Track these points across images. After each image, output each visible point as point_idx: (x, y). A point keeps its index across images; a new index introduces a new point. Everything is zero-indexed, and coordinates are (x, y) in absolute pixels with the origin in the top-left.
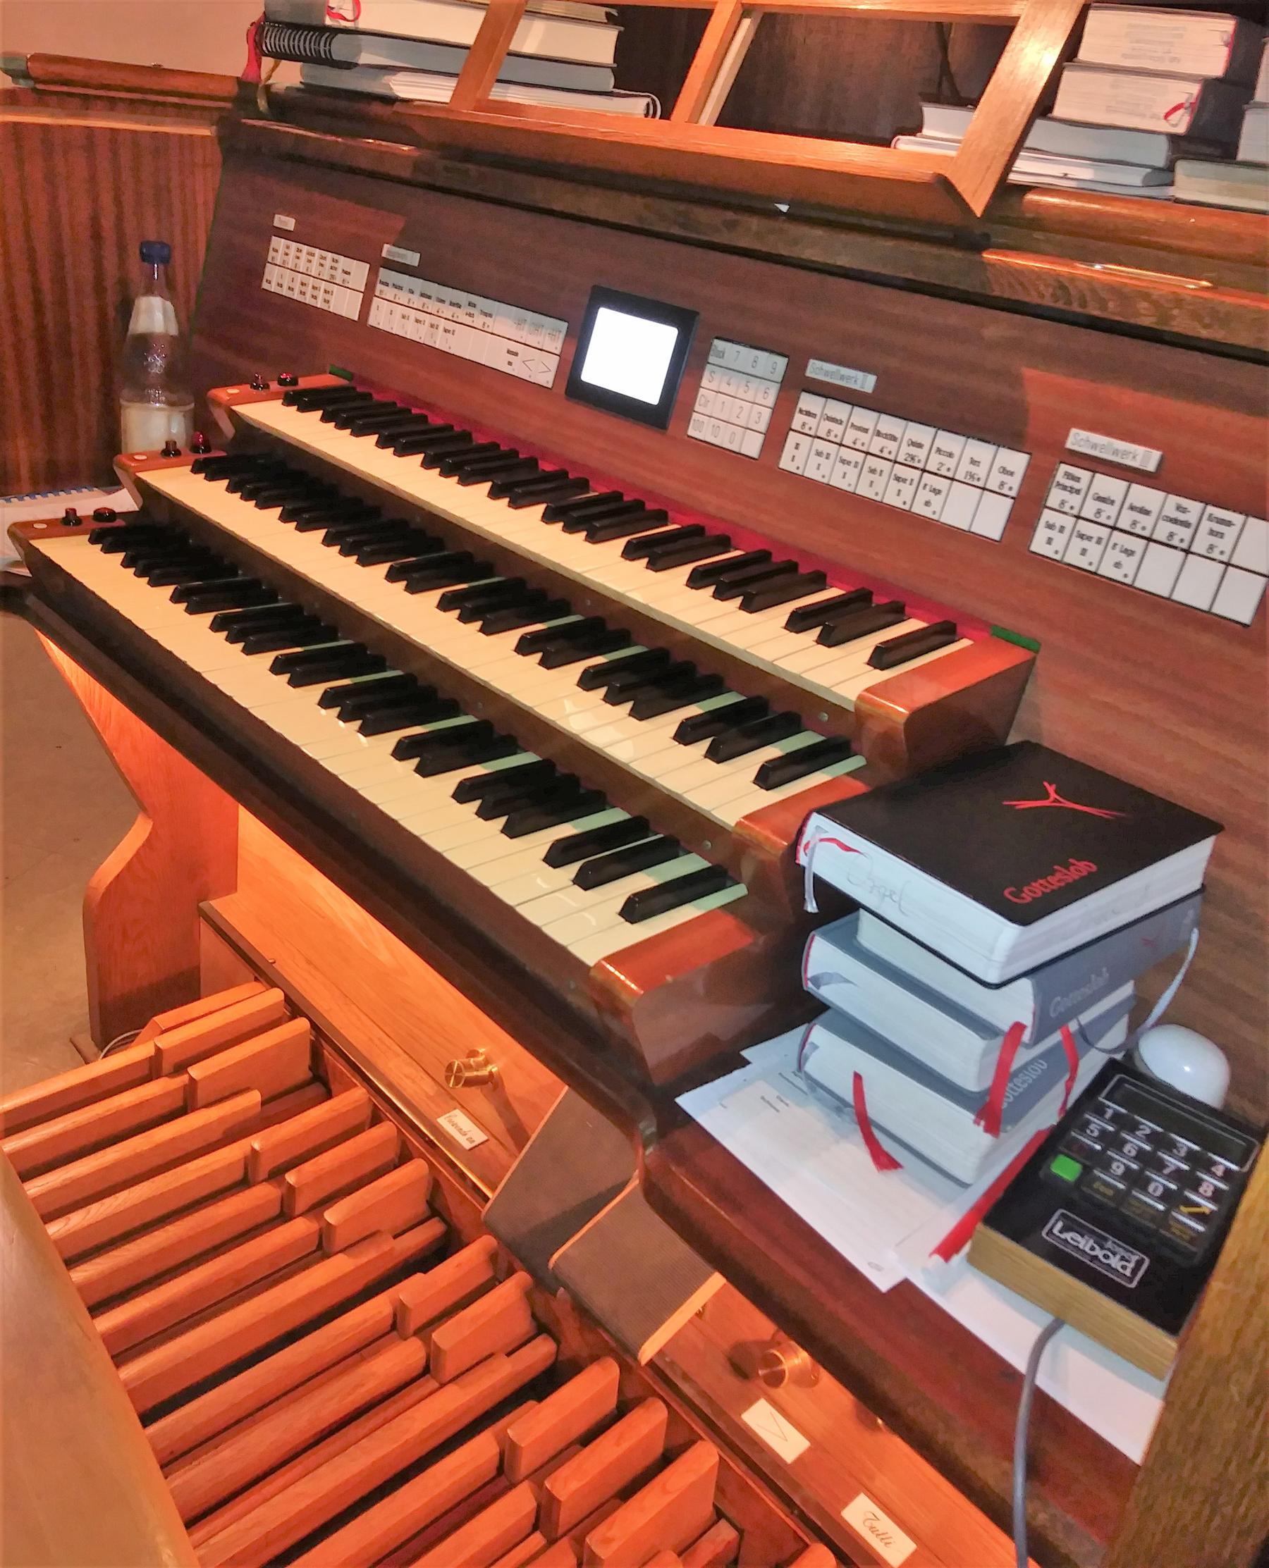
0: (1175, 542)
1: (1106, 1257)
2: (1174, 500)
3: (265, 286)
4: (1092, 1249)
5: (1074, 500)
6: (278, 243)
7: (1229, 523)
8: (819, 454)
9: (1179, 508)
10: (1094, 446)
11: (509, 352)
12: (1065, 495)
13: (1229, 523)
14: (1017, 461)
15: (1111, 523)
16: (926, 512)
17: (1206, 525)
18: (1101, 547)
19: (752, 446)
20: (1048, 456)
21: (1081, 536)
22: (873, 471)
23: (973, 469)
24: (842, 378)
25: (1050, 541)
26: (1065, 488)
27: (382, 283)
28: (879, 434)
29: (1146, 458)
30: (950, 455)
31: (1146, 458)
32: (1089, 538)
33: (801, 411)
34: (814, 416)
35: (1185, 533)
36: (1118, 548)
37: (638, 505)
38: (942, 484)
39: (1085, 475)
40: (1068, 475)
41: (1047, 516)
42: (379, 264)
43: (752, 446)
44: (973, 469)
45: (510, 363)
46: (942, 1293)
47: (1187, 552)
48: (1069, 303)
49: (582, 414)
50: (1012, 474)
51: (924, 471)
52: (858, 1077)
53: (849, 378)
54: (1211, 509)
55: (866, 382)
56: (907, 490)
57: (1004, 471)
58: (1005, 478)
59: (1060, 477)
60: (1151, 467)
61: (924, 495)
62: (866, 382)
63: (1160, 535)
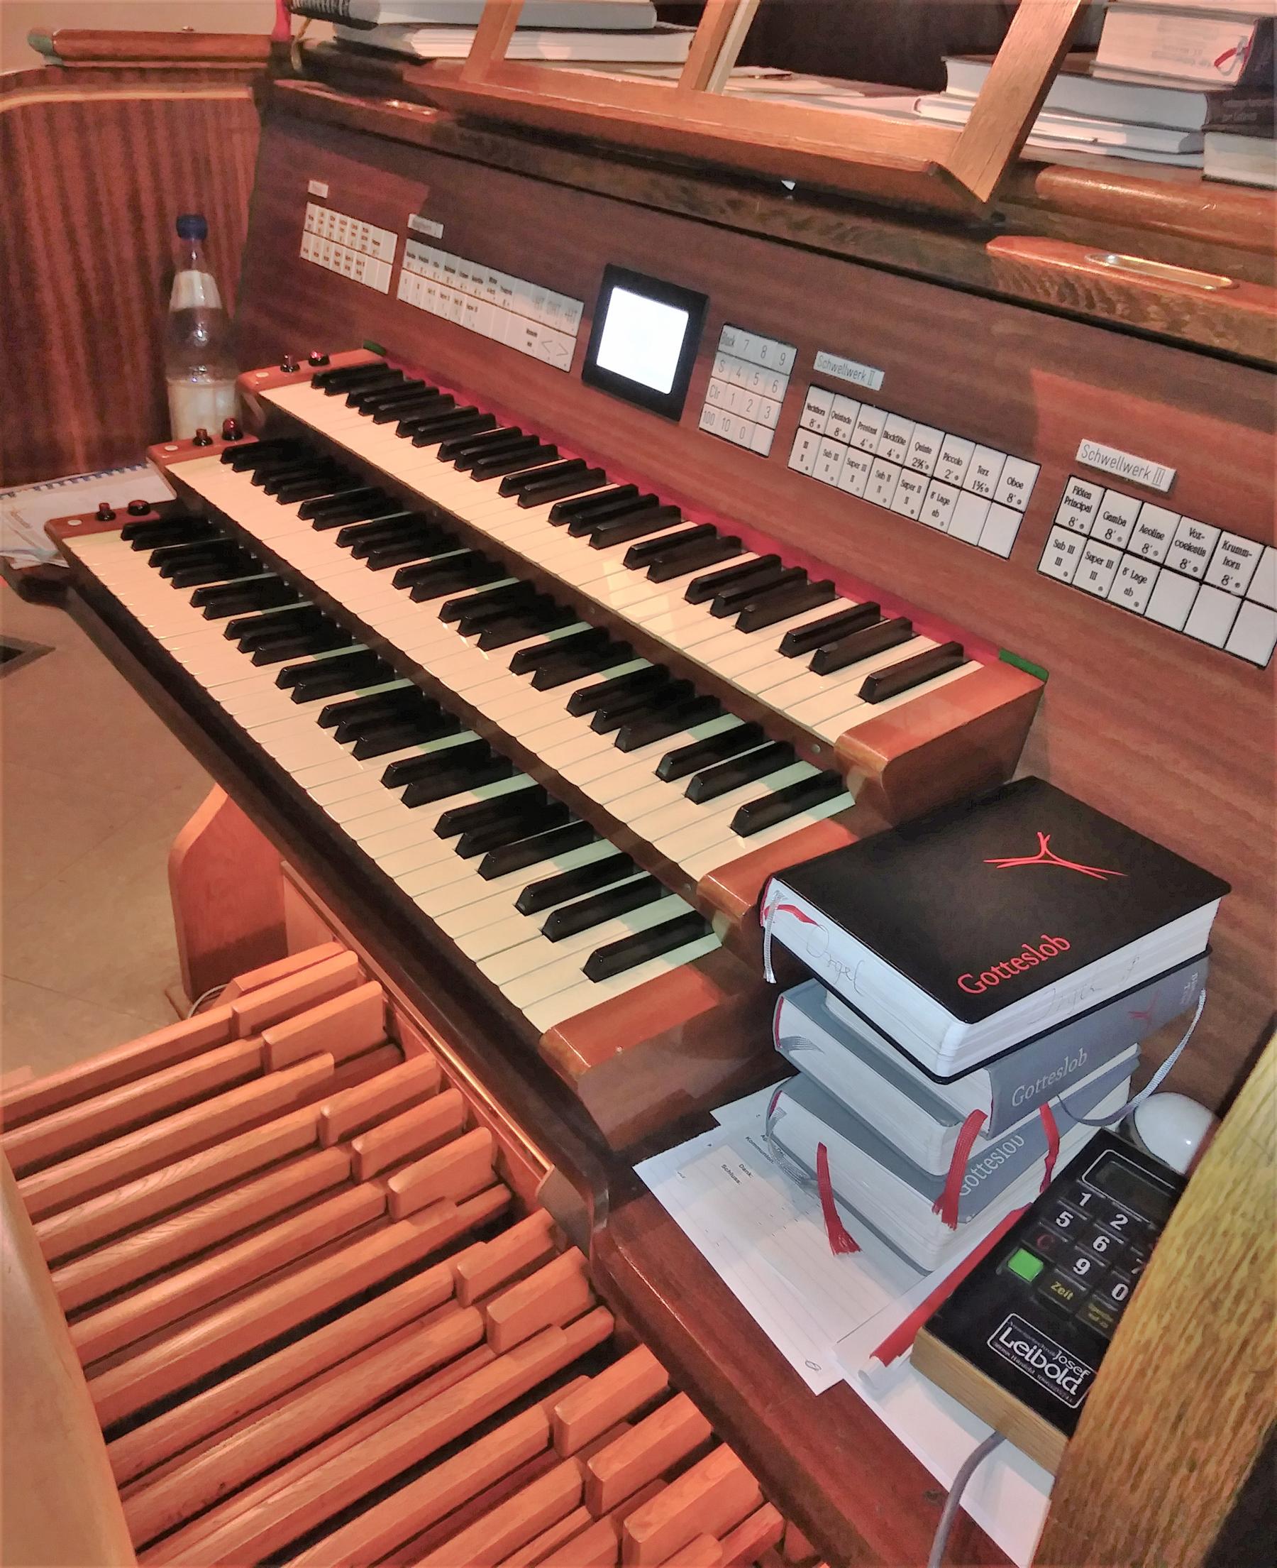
0: (1189, 570)
1: (1052, 1371)
2: (1188, 523)
3: (303, 255)
4: (1039, 1361)
5: (1084, 519)
6: (313, 210)
7: (1245, 553)
8: (827, 454)
9: (1192, 533)
10: (1105, 460)
11: (528, 332)
12: (1075, 512)
13: (1245, 553)
14: (1026, 472)
15: (1122, 545)
16: (934, 523)
17: (1221, 554)
18: (1112, 571)
19: (761, 442)
20: (1058, 468)
21: (1091, 558)
22: (881, 476)
23: (981, 478)
24: (850, 373)
25: (1059, 561)
26: (1075, 504)
27: (409, 255)
28: (886, 435)
29: (1159, 476)
30: (959, 462)
31: (1159, 476)
32: (1100, 561)
33: (809, 407)
34: (822, 412)
35: (1200, 562)
36: (1129, 573)
37: (653, 500)
38: (950, 493)
39: (1096, 491)
40: (1079, 491)
42: (407, 234)
44: (981, 478)
45: (529, 344)
46: (877, 1398)
47: (1202, 582)
48: (1076, 302)
49: (599, 401)
50: (1020, 486)
51: (932, 478)
52: (822, 1148)
53: (856, 374)
54: (1226, 536)
56: (916, 498)
57: (1013, 482)
58: (1014, 490)
59: (1069, 493)
60: (1164, 487)
61: (931, 504)
62: (873, 379)
63: (1173, 562)
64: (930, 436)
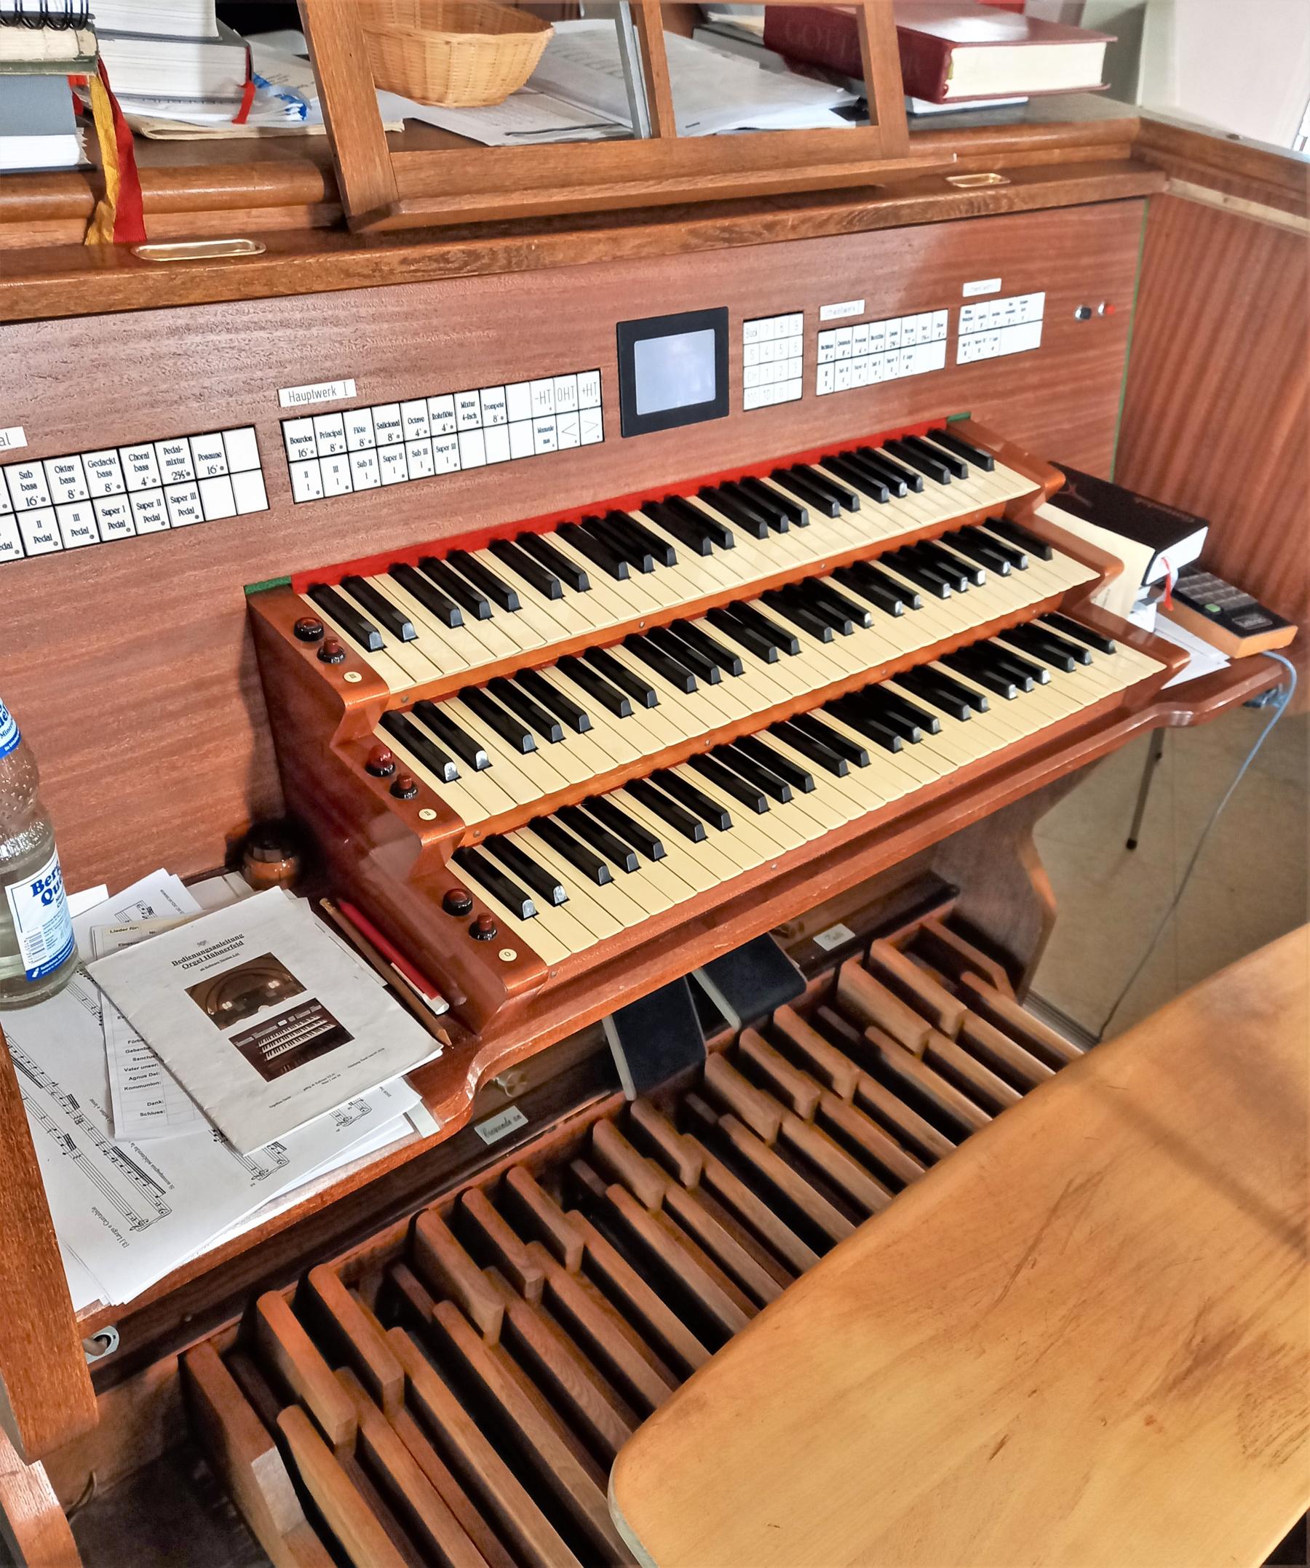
19: (794, 391)
41: (961, 340)
43: (794, 391)
55: (857, 308)
64: (894, 325)
